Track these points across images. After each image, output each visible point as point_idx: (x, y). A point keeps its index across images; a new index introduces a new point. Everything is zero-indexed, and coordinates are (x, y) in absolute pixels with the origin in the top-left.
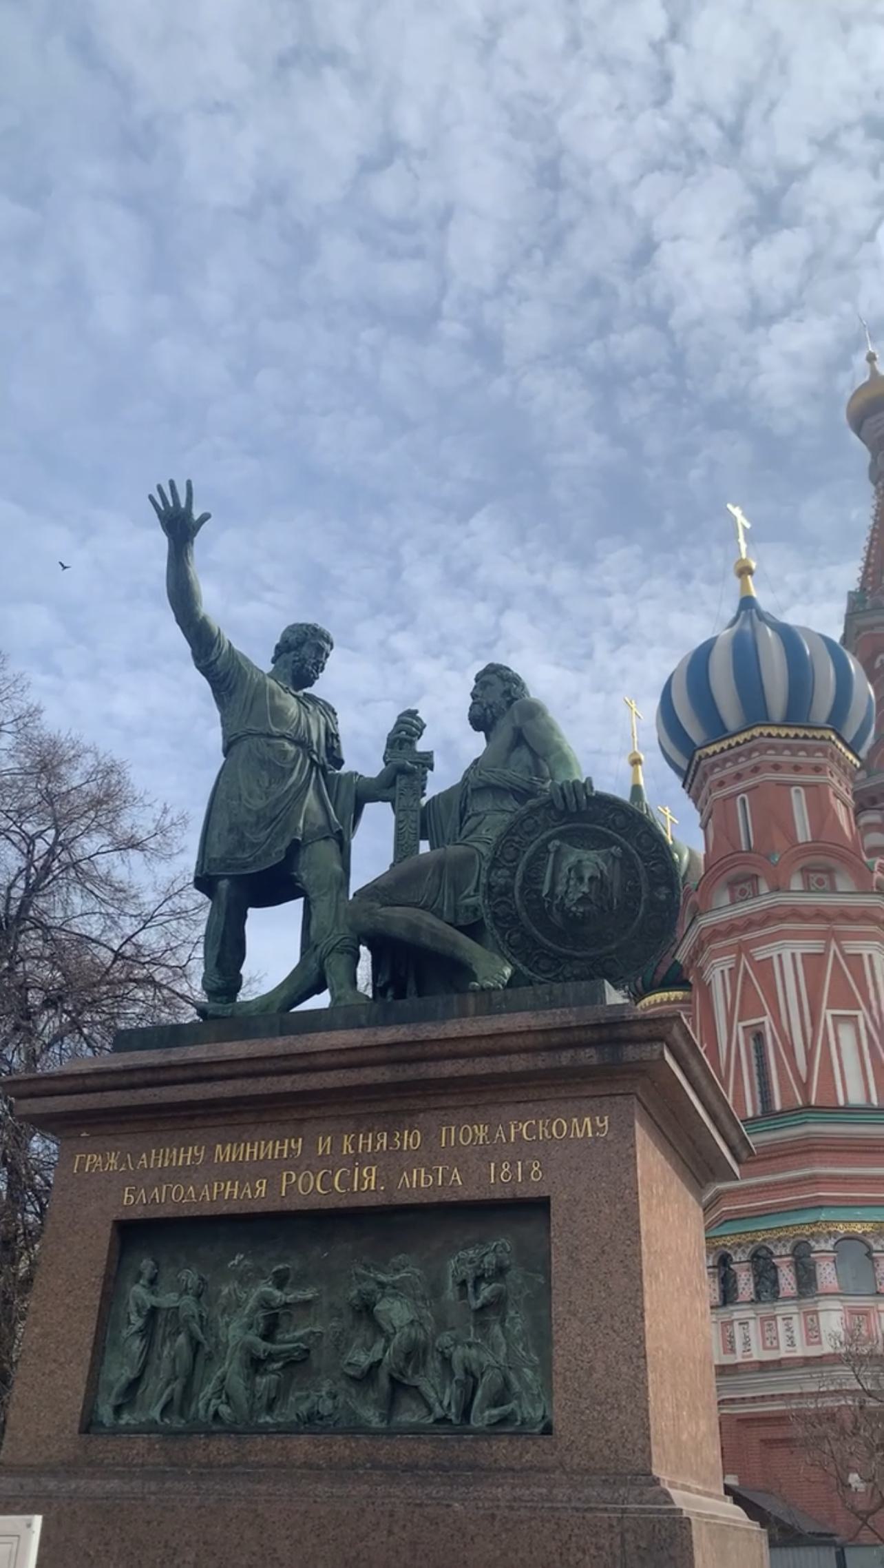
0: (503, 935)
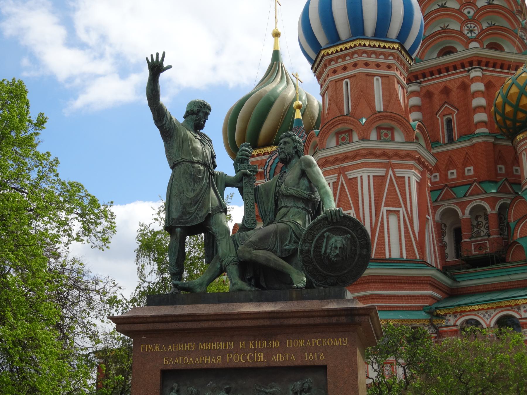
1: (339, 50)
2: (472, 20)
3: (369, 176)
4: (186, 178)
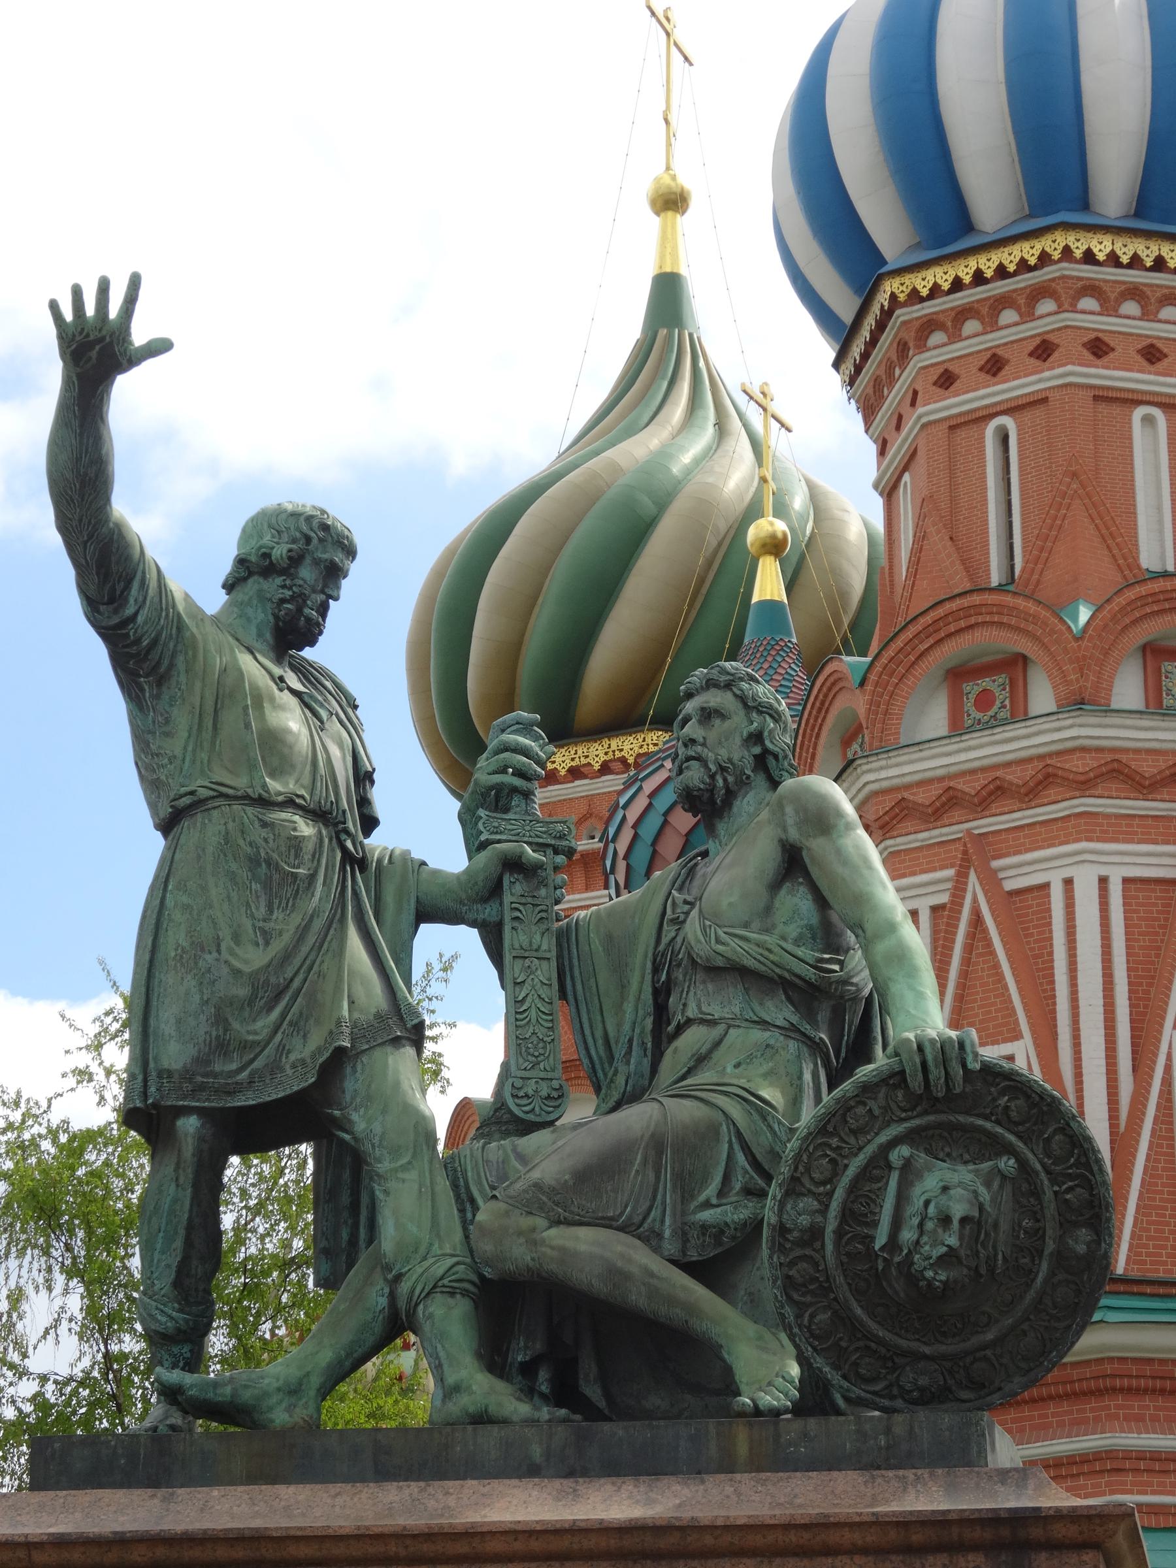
0: (798, 1316)
1: (967, 279)
3: (1103, 881)
4: (232, 876)
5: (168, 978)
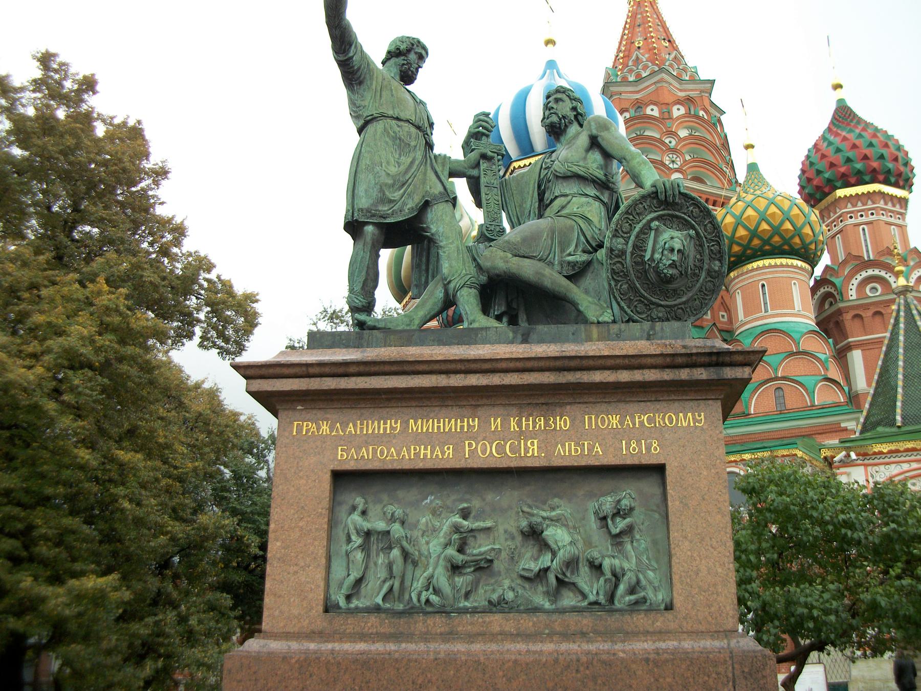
2: (674, 151)
4: (387, 143)
5: (361, 176)
